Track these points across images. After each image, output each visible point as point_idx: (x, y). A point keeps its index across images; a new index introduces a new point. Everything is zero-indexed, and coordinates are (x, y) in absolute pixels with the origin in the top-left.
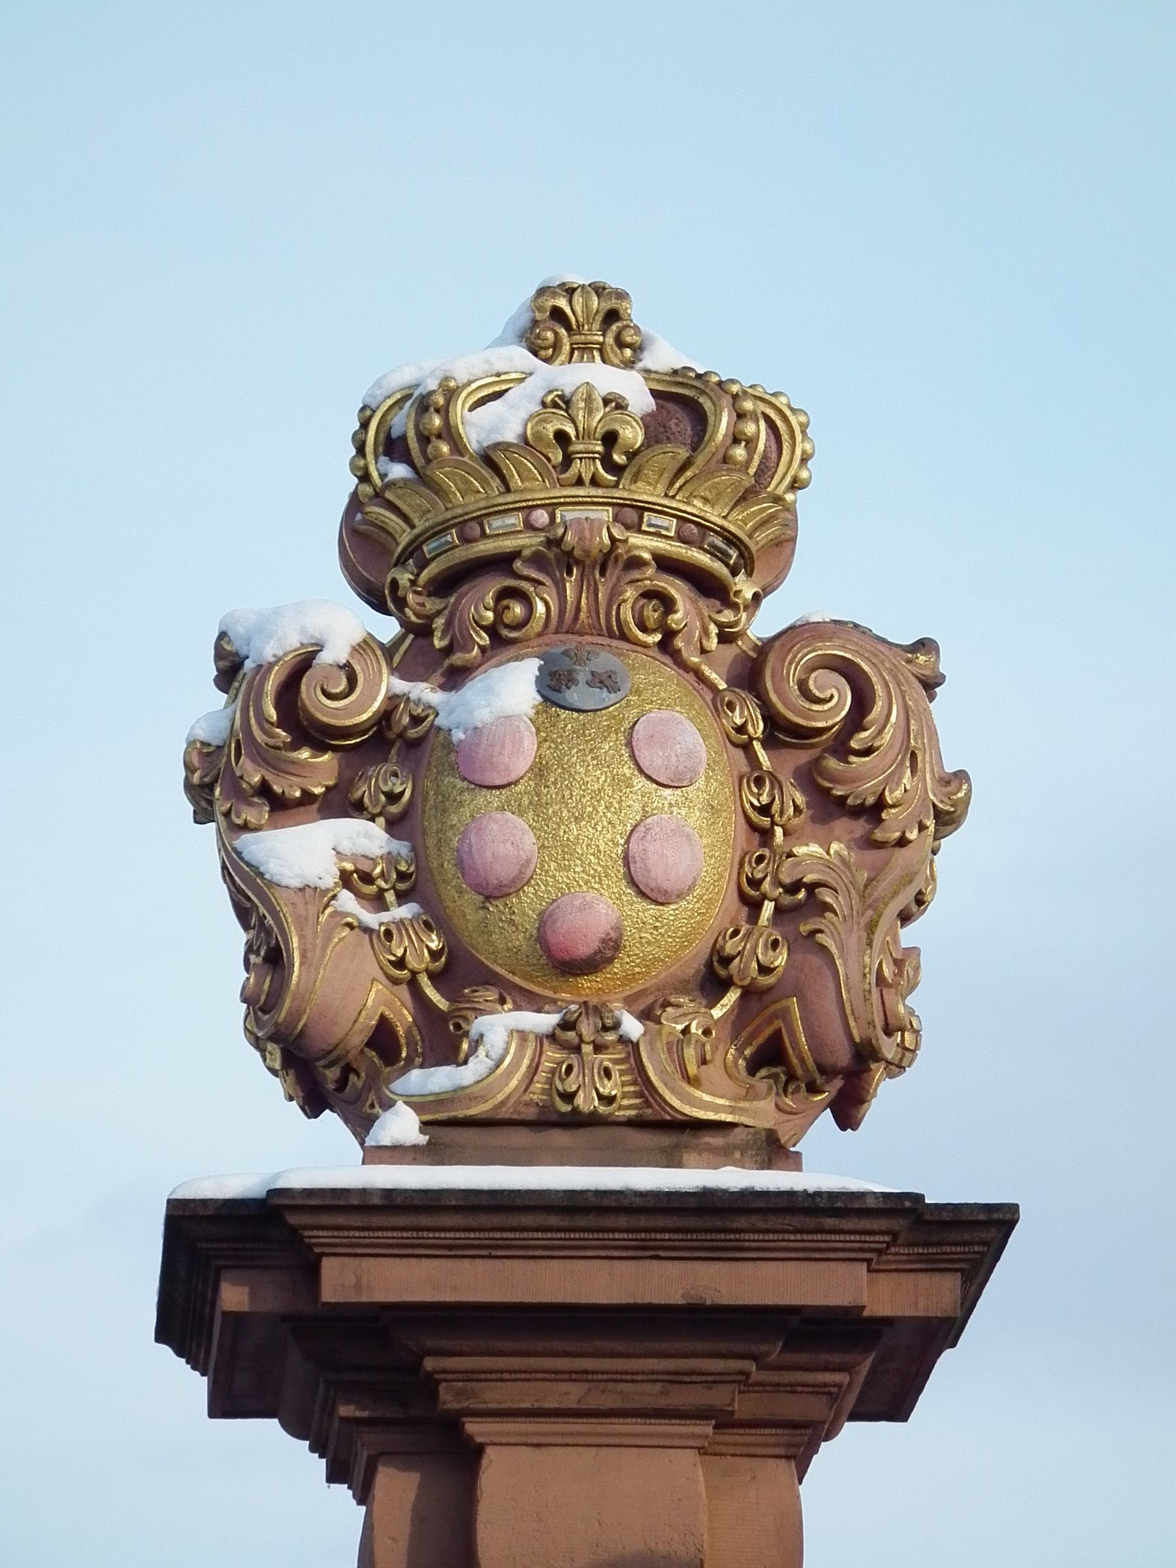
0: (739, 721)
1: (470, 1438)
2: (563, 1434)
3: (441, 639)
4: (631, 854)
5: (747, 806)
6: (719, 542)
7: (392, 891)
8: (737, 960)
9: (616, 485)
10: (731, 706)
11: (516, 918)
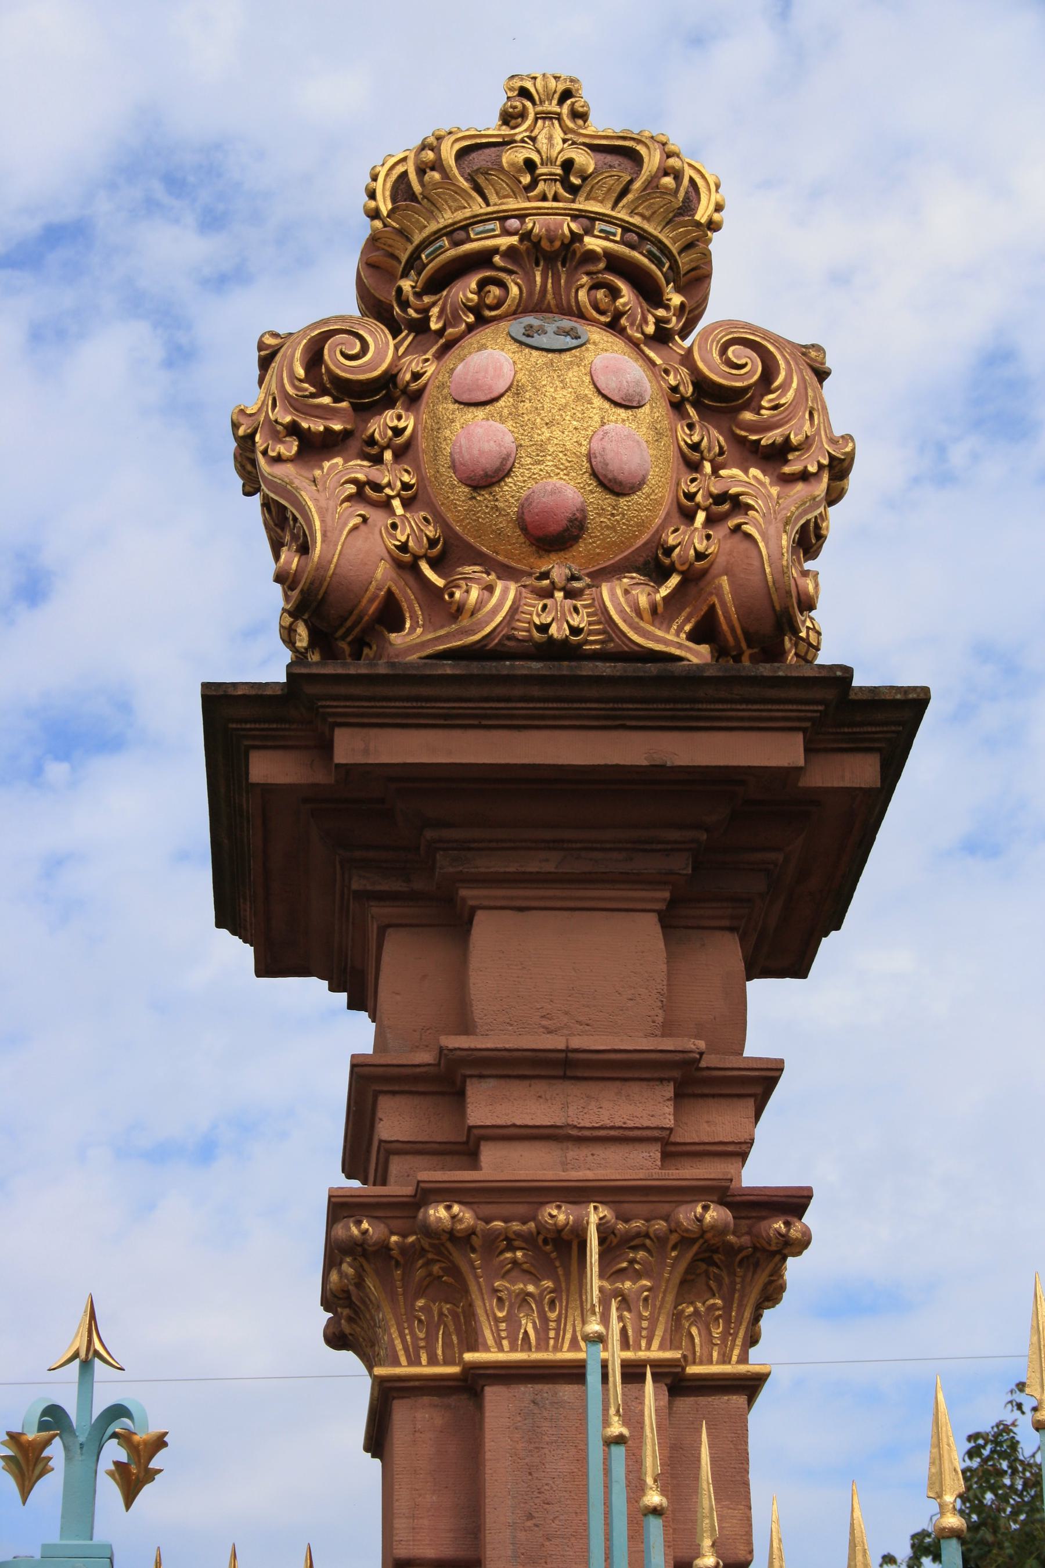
0: (673, 383)
1: (464, 900)
2: (542, 898)
3: (436, 323)
4: (592, 452)
5: (682, 443)
6: (654, 250)
7: (398, 499)
8: (678, 550)
9: (573, 201)
10: (667, 372)
11: (500, 505)
